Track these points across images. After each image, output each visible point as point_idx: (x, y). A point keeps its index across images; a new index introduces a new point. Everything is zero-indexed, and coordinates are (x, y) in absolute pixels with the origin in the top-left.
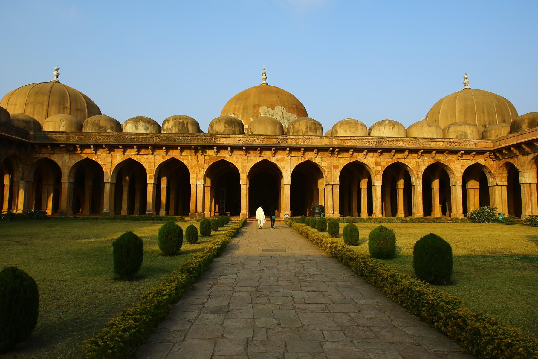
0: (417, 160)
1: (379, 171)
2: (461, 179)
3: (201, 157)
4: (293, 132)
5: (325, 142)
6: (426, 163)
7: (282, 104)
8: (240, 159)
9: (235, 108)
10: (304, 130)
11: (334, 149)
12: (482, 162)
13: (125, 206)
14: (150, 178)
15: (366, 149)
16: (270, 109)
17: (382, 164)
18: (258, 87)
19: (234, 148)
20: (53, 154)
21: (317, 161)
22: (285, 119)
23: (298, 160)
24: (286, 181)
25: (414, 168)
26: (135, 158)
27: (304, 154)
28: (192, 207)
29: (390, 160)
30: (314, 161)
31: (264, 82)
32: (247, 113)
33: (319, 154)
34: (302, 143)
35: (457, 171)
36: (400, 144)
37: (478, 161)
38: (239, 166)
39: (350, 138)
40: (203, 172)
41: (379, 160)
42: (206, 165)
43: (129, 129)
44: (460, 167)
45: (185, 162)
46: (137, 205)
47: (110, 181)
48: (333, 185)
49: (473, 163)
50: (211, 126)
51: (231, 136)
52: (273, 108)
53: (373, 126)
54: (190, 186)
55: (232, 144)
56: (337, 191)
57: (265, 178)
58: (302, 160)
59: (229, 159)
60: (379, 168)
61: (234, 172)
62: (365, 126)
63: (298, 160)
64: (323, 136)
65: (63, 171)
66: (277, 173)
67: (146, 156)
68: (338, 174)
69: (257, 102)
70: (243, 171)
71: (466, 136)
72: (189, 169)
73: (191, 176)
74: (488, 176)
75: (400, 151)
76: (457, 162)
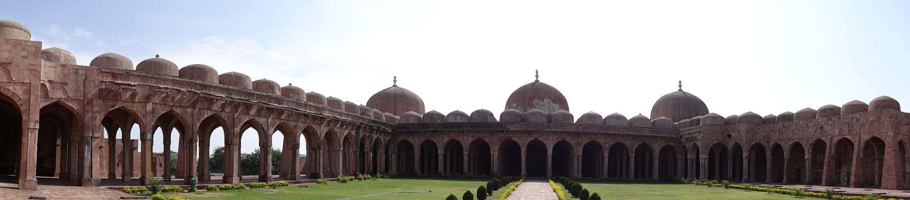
11: (579, 133)
21: (568, 140)
24: (550, 153)
38: (520, 143)
40: (497, 147)
43: (451, 120)
56: (580, 159)
59: (514, 139)
75: (623, 135)
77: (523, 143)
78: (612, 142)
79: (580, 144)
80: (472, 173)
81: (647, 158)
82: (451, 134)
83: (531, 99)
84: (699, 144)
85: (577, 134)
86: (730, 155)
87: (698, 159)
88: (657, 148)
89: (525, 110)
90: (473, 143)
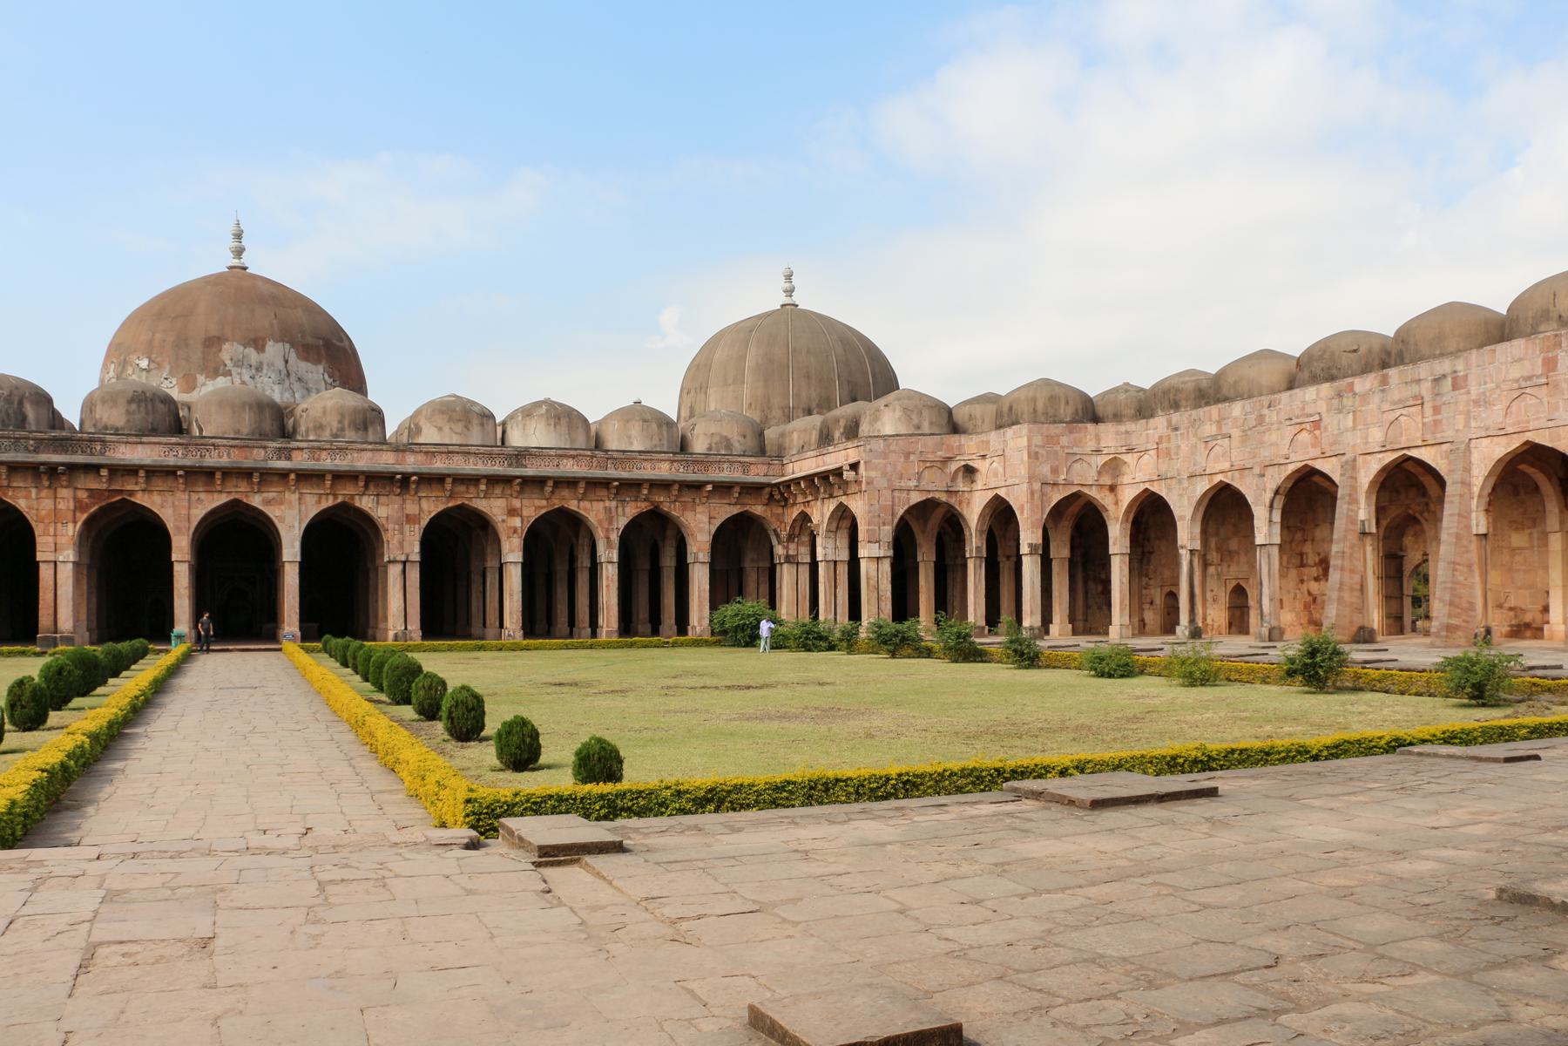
0: (607, 503)
1: (515, 531)
2: (707, 546)
3: (65, 493)
4: (307, 431)
5: (386, 461)
6: (628, 510)
7: (286, 335)
8: (170, 499)
9: (150, 342)
10: (335, 425)
11: (406, 477)
12: (758, 510)
15: (485, 477)
16: (252, 353)
17: (525, 513)
18: (220, 276)
19: (154, 472)
21: (365, 503)
22: (293, 378)
23: (319, 502)
25: (600, 522)
27: (332, 486)
28: (44, 619)
29: (544, 503)
30: (357, 504)
31: (236, 262)
32: (187, 360)
33: (372, 489)
34: (327, 462)
35: (701, 530)
36: (570, 468)
39: (446, 450)
40: (71, 531)
41: (516, 503)
44: (706, 519)
45: (22, 504)
48: (404, 563)
49: (736, 510)
50: (89, 405)
51: (145, 439)
52: (260, 348)
53: (512, 417)
54: (35, 566)
55: (147, 461)
57: (236, 544)
58: (328, 503)
59: (140, 499)
60: (517, 522)
61: (154, 533)
62: (491, 416)
63: (319, 502)
64: (384, 442)
69: (214, 330)
70: (178, 528)
71: (729, 446)
72: (33, 524)
73: (39, 540)
74: (774, 542)
75: (571, 483)
76: (699, 509)
77: (181, 515)
78: (533, 508)
79: (410, 519)
81: (668, 562)
83: (213, 343)
84: (857, 506)
85: (400, 483)
86: (974, 543)
87: (854, 563)
88: (700, 526)
89: (190, 386)
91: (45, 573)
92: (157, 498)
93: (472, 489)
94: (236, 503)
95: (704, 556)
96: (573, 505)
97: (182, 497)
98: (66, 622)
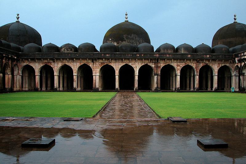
3: (97, 63)
12: (228, 65)
13: (44, 85)
14: (75, 73)
20: (30, 63)
26: (67, 64)
28: (94, 86)
29: (184, 64)
37: (225, 64)
38: (114, 67)
40: (98, 70)
41: (179, 64)
42: (99, 67)
45: (90, 66)
46: (49, 85)
47: (56, 75)
61: (112, 70)
65: (35, 71)
66: (132, 70)
67: (72, 63)
68: (160, 71)
80: (79, 89)
82: (64, 61)
90: (80, 68)
91: (94, 77)
92: (113, 64)
93: (170, 61)
94: (126, 64)
95: (217, 74)
96: (190, 64)
97: (117, 63)
98: (97, 87)
